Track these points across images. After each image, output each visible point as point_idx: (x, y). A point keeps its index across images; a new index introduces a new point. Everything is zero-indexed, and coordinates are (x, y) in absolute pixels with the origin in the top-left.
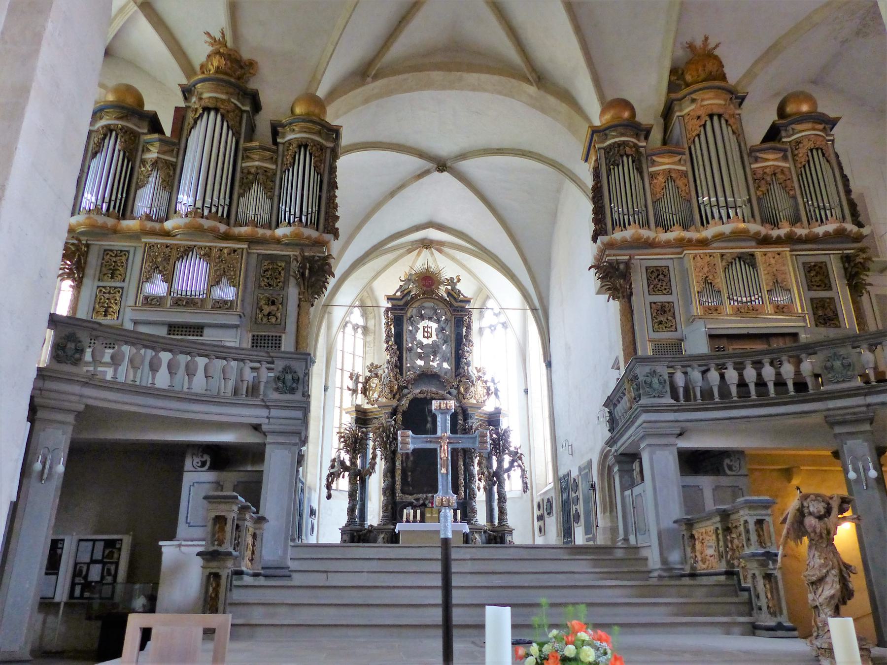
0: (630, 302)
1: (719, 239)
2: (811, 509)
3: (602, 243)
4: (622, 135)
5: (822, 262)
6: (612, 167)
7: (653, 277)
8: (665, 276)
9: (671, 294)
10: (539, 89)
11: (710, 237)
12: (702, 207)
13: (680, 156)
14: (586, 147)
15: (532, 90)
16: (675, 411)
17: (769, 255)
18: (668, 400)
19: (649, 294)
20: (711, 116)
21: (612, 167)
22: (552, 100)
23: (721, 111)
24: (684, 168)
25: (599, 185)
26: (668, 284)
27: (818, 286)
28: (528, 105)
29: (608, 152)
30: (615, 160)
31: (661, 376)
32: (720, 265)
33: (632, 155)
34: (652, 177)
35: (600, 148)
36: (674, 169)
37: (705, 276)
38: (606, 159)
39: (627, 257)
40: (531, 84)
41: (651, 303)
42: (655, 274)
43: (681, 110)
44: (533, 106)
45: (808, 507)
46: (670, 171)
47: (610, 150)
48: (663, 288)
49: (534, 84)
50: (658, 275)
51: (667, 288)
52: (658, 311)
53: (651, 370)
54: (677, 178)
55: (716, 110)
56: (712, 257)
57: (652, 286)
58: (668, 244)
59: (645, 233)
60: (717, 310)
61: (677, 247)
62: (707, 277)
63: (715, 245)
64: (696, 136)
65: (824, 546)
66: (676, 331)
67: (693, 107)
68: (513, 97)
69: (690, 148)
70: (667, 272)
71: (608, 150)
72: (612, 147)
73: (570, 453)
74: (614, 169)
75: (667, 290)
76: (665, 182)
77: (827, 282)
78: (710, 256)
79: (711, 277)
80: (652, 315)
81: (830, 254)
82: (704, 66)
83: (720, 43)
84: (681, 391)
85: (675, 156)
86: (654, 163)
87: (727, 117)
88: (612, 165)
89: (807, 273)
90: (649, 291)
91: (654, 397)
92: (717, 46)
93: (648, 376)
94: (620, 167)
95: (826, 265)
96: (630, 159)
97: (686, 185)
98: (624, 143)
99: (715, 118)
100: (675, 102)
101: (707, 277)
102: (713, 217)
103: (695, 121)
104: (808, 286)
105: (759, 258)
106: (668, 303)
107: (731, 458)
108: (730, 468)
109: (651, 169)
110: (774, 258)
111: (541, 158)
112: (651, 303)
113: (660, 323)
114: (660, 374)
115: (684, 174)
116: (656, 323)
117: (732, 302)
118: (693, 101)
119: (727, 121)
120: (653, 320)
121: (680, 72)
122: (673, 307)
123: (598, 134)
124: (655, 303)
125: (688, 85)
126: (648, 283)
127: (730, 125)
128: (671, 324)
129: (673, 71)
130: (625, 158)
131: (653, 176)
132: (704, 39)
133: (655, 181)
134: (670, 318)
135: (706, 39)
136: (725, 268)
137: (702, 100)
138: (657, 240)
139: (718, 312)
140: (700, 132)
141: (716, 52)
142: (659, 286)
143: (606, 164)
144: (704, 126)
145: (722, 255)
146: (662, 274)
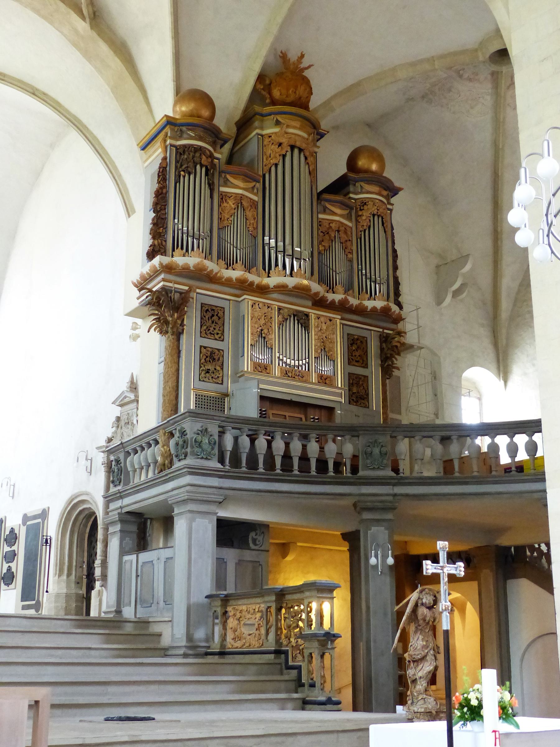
0: (178, 340)
1: (280, 291)
2: (424, 601)
3: (161, 264)
4: (200, 139)
6: (182, 173)
7: (207, 317)
8: (219, 318)
9: (223, 340)
10: (92, 28)
11: (271, 286)
12: (266, 248)
13: (254, 184)
14: (151, 133)
15: (82, 26)
16: (221, 477)
17: (322, 319)
18: (215, 464)
19: (201, 336)
20: (292, 147)
21: (182, 173)
22: (103, 48)
23: (303, 146)
24: (255, 198)
25: (164, 191)
26: (221, 329)
27: (357, 361)
28: (69, 41)
29: (181, 154)
30: (187, 167)
31: (211, 435)
32: (276, 319)
33: (206, 167)
34: (222, 199)
35: (171, 145)
36: (247, 197)
37: (260, 328)
38: (177, 162)
39: (187, 288)
40: (83, 18)
41: (201, 347)
42: (210, 314)
43: (262, 128)
44: (75, 45)
45: (422, 599)
46: (242, 197)
47: (184, 152)
48: (215, 331)
49: (88, 20)
50: (213, 316)
51: (220, 332)
52: (207, 357)
53: (202, 427)
54: (248, 208)
55: (298, 144)
56: (270, 309)
57: (205, 327)
58: (228, 283)
59: (211, 266)
60: (266, 369)
61: (236, 288)
62: (262, 330)
63: (275, 296)
64: (274, 164)
65: (427, 631)
66: (222, 384)
67: (277, 130)
68: (51, 23)
69: (264, 176)
70: (222, 314)
71: (181, 151)
72: (186, 149)
73: (11, 495)
74: (184, 177)
75: (219, 335)
76: (235, 209)
78: (268, 307)
79: (265, 331)
80: (200, 360)
81: (371, 330)
82: (296, 88)
83: (312, 65)
84: (228, 455)
85: (251, 182)
86: (226, 183)
87: (307, 154)
88: (184, 171)
89: (350, 345)
90: (201, 332)
91: (202, 458)
92: (309, 67)
93: (198, 434)
94: (192, 177)
95: (366, 341)
96: (204, 170)
97: (254, 219)
98: (200, 148)
99: (296, 151)
100: (257, 116)
101: (262, 330)
102: (277, 265)
103: (274, 147)
104: (349, 359)
105: (313, 321)
106: (219, 350)
107: (257, 532)
108: (254, 541)
109: (223, 189)
110: (325, 323)
111: (58, 108)
112: (201, 347)
113: (208, 371)
114: (210, 434)
115: (254, 204)
116: (203, 370)
117: (281, 362)
118: (278, 123)
119: (306, 158)
120: (200, 367)
121: (268, 82)
122: (223, 357)
123: (172, 127)
124: (205, 348)
125: (274, 102)
126: (201, 322)
127: (308, 163)
128: (218, 375)
129: (261, 78)
130: (198, 167)
131: (223, 197)
132: (300, 55)
133: (225, 204)
134: (218, 368)
135: (302, 56)
136: (280, 324)
137: (288, 126)
138: (218, 275)
139: (268, 371)
140: (279, 162)
141: (306, 73)
142: (212, 329)
143: (176, 167)
144: (284, 156)
145: (280, 309)
146: (217, 315)
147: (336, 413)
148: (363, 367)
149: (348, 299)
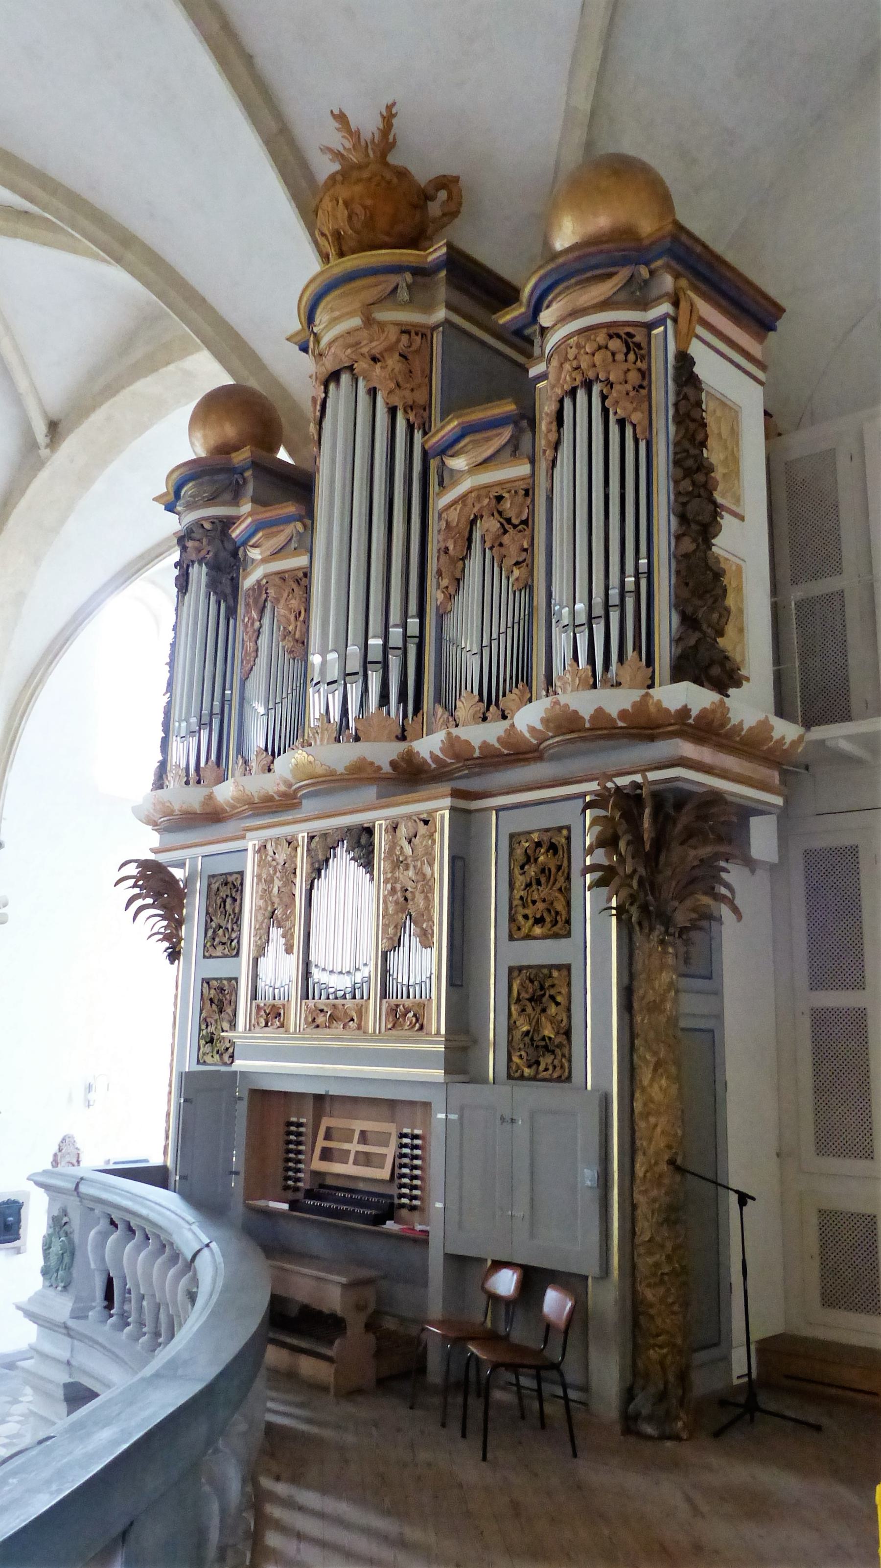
5: (559, 829)
8: (235, 900)
17: (403, 831)
19: (205, 957)
27: (539, 921)
51: (234, 935)
77: (559, 906)
89: (517, 871)
95: (568, 838)
104: (512, 919)
105: (381, 841)
106: (230, 979)
112: (203, 980)
120: (200, 1030)
147: (432, 1121)
148: (556, 936)
149: (457, 737)
